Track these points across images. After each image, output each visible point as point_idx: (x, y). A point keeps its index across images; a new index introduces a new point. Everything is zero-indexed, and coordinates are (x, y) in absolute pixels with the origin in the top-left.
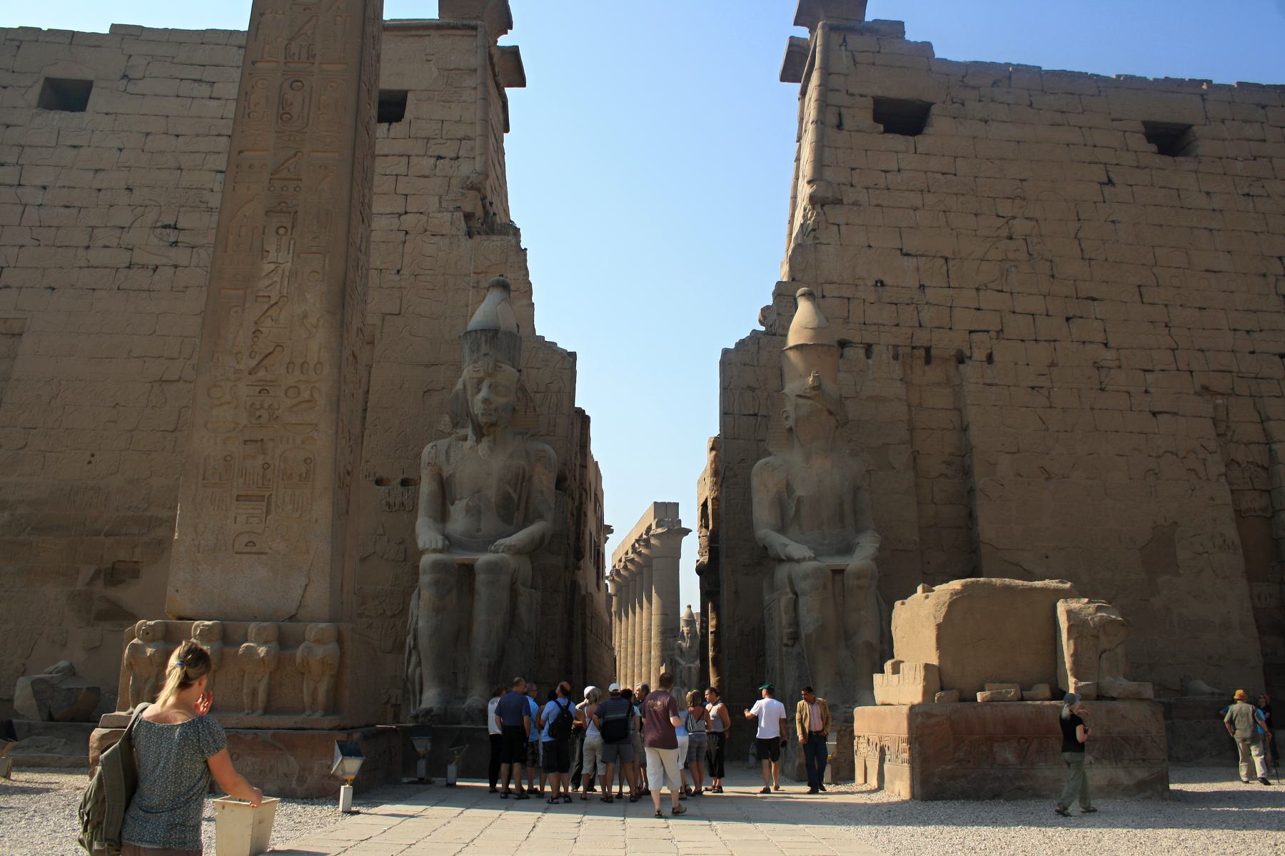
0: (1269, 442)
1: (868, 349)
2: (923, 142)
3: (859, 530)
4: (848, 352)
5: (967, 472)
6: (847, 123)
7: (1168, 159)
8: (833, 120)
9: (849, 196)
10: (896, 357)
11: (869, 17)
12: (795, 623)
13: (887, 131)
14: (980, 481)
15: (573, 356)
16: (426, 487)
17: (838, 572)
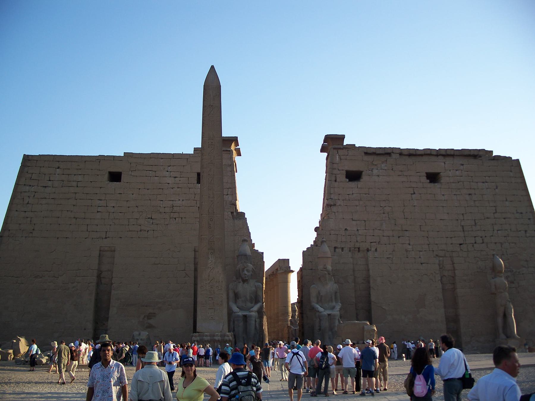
0: (454, 270)
1: (342, 249)
2: (360, 184)
3: (336, 302)
4: (337, 250)
5: (369, 282)
6: (338, 180)
7: (432, 184)
8: (334, 179)
9: (339, 203)
10: (350, 251)
11: (345, 144)
12: (320, 326)
13: (350, 181)
14: (372, 284)
15: (263, 253)
16: (231, 295)
17: (329, 315)
